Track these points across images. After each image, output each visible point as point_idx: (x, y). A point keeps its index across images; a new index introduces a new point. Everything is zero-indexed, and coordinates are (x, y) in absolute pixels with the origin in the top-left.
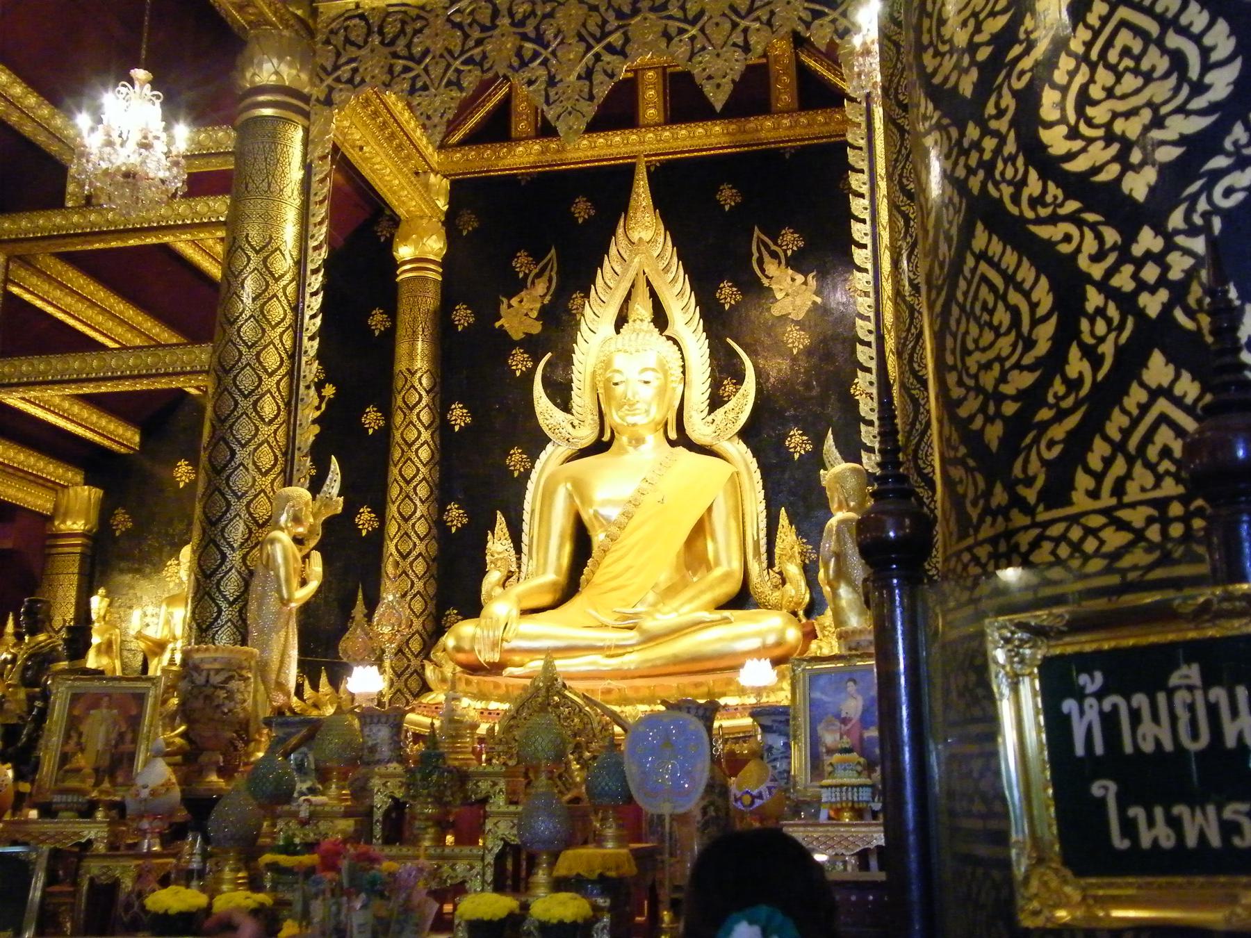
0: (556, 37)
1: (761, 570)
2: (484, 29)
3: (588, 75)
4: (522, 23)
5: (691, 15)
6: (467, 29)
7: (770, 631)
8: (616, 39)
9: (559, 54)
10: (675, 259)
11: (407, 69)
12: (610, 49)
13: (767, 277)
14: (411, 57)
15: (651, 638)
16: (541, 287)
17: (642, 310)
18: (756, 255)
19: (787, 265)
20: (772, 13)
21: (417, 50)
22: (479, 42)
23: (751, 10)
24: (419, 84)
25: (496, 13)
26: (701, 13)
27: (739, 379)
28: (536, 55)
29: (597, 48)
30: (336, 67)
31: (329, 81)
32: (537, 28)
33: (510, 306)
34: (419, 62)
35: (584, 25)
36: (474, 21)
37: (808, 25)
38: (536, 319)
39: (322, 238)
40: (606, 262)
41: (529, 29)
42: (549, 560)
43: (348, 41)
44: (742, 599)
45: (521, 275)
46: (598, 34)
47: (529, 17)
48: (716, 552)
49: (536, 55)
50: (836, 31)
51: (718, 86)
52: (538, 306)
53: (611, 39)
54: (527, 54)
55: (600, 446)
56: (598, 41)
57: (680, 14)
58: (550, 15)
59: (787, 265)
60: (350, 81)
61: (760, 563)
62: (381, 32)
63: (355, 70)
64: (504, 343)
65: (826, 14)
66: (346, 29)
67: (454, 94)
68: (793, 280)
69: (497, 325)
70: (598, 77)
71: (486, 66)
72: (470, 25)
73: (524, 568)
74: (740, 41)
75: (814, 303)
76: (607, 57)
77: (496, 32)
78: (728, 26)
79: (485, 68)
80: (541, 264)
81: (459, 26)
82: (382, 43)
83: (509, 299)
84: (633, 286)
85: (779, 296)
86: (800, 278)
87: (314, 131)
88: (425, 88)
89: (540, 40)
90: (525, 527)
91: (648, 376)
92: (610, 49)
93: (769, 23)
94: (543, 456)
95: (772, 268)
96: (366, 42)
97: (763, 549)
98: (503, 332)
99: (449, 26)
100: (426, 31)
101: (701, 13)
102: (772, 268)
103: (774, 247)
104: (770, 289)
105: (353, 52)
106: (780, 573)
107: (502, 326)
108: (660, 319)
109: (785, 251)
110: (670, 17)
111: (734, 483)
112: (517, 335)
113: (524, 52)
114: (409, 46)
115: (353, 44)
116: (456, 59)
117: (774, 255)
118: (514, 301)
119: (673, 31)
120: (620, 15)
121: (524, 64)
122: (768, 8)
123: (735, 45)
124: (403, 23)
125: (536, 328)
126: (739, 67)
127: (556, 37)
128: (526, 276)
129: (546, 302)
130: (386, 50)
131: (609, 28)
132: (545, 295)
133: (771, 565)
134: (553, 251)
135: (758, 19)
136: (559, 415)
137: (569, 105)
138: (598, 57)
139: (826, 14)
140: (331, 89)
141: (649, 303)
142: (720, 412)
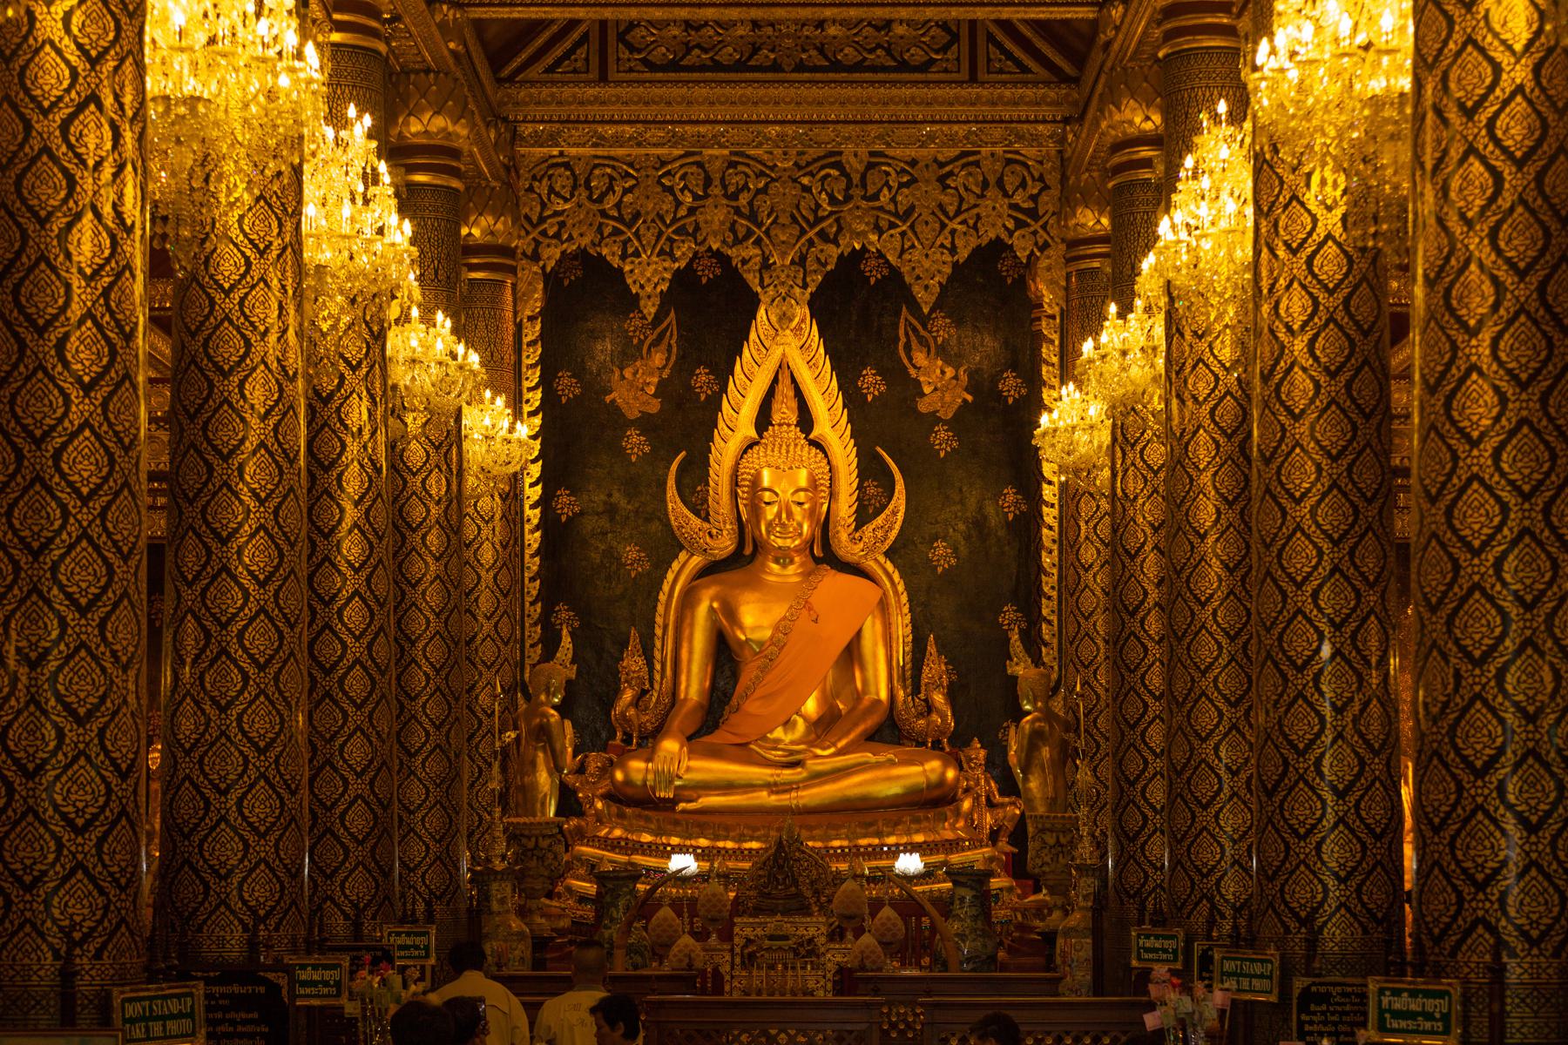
0: (769, 216)
1: (907, 695)
2: (696, 197)
3: (801, 261)
4: (734, 196)
5: (901, 209)
6: (678, 193)
7: (933, 770)
8: (829, 226)
9: (773, 233)
10: (822, 350)
11: (616, 232)
12: (822, 235)
13: (914, 366)
14: (620, 219)
16: (658, 359)
17: (785, 411)
18: (903, 340)
19: (937, 354)
20: (978, 217)
21: (627, 213)
22: (692, 211)
23: (958, 212)
24: (630, 250)
25: (708, 182)
26: (912, 208)
28: (750, 233)
29: (811, 234)
30: (542, 220)
31: (535, 234)
32: (750, 203)
33: (623, 378)
34: (629, 227)
35: (798, 207)
36: (685, 187)
37: (1011, 233)
38: (655, 396)
39: (537, 404)
40: (746, 350)
41: (743, 200)
42: (694, 684)
43: (551, 190)
44: (889, 731)
45: (635, 341)
46: (811, 218)
47: (742, 190)
48: (865, 682)
49: (750, 233)
50: (1036, 244)
51: (926, 287)
52: (656, 380)
53: (824, 225)
54: (741, 232)
56: (812, 226)
57: (891, 207)
58: (764, 190)
59: (937, 354)
60: (557, 236)
61: (905, 688)
62: (588, 187)
63: (562, 225)
64: (616, 420)
65: (1028, 225)
66: (550, 177)
67: (666, 264)
68: (943, 373)
69: (608, 399)
70: (811, 265)
71: (700, 238)
72: (682, 190)
73: (657, 686)
74: (947, 243)
75: (965, 400)
76: (820, 245)
77: (709, 201)
78: (937, 226)
79: (700, 238)
80: (658, 330)
81: (670, 190)
82: (590, 198)
83: (622, 369)
84: (775, 380)
85: (927, 390)
86: (950, 372)
87: (522, 287)
88: (637, 254)
89: (753, 217)
90: (658, 644)
91: (802, 496)
92: (822, 235)
93: (975, 227)
94: (676, 566)
95: (920, 358)
96: (572, 195)
97: (908, 674)
99: (659, 189)
100: (637, 192)
101: (912, 208)
102: (920, 358)
103: (922, 332)
104: (918, 384)
105: (561, 206)
106: (926, 701)
107: (613, 401)
108: (806, 421)
109: (935, 338)
110: (881, 209)
111: (883, 606)
112: (633, 414)
113: (738, 227)
114: (618, 206)
115: (558, 195)
116: (668, 227)
117: (923, 342)
118: (628, 373)
119: (883, 224)
120: (832, 200)
121: (738, 242)
122: (975, 211)
123: (942, 246)
124: (612, 178)
125: (654, 407)
126: (948, 270)
127: (769, 216)
128: (641, 342)
129: (665, 376)
130: (595, 207)
131: (820, 213)
132: (664, 367)
133: (916, 690)
134: (672, 314)
135: (964, 222)
136: (696, 521)
137: (783, 291)
138: (811, 243)
139: (1028, 225)
140: (537, 243)
141: (794, 404)
142: (868, 529)
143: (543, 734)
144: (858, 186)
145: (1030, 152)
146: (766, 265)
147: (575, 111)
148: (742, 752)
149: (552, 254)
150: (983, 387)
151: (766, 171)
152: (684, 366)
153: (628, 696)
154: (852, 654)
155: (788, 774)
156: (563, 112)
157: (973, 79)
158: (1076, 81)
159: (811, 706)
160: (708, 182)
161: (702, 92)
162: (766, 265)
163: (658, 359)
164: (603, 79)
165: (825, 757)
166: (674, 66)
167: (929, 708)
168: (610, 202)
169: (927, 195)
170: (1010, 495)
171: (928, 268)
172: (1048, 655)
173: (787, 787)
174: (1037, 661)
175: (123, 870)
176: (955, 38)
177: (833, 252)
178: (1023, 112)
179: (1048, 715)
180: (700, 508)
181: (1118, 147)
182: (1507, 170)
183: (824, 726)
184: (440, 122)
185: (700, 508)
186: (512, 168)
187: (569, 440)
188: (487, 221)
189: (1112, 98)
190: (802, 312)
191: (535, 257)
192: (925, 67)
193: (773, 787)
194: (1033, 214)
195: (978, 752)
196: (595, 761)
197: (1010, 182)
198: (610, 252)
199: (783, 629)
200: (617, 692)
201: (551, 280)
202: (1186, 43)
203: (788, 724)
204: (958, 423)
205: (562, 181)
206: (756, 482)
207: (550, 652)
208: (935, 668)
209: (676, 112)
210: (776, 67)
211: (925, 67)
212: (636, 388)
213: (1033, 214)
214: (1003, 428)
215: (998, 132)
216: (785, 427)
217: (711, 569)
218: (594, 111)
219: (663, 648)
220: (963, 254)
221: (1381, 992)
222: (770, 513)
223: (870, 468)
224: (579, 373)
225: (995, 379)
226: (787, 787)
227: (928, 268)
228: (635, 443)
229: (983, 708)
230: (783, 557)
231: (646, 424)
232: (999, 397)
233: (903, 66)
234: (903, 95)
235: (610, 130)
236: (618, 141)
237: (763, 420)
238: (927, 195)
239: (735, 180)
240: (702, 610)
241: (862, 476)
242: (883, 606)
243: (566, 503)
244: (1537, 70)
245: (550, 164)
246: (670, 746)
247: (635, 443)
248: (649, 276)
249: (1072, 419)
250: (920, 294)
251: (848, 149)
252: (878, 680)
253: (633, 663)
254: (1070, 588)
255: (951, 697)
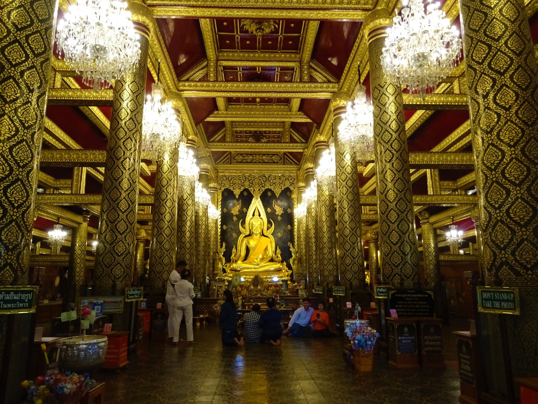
3: (259, 190)
8: (263, 185)
15: (261, 267)
16: (238, 206)
17: (257, 213)
27: (272, 225)
41: (251, 181)
42: (243, 253)
44: (272, 260)
55: (250, 235)
89: (252, 184)
95: (276, 206)
98: (232, 214)
102: (276, 206)
108: (260, 215)
111: (271, 242)
143: (220, 259)
144: (267, 179)
145: (292, 175)
146: (254, 190)
147: (227, 168)
148: (250, 263)
149: (223, 189)
150: (285, 210)
151: (254, 177)
152: (242, 208)
153: (233, 255)
154: (266, 249)
155: (257, 266)
156: (225, 168)
157: (284, 164)
158: (299, 165)
159: (260, 256)
160: (246, 179)
161: (245, 166)
162: (254, 190)
163: (238, 206)
164: (231, 164)
165: (263, 264)
166: (241, 162)
167: (278, 257)
168: (231, 181)
169: (277, 181)
170: (289, 226)
171: (278, 191)
172: (296, 247)
173: (257, 268)
174: (294, 248)
175: (128, 264)
176: (281, 159)
177: (264, 189)
178: (291, 169)
179: (296, 256)
180: (244, 228)
181: (306, 170)
182: (393, 133)
183: (262, 259)
184: (206, 165)
185: (244, 228)
186: (217, 177)
187: (226, 217)
188: (214, 184)
189: (306, 162)
190: (259, 199)
191: (220, 189)
192: (277, 163)
193: (255, 268)
194: (293, 183)
195: (285, 263)
196: (228, 265)
197: (290, 179)
198: (231, 188)
199: (256, 245)
200: (231, 254)
201: (223, 193)
202: (319, 147)
203: (257, 259)
204: (282, 216)
205: (225, 179)
206: (252, 224)
207: (221, 247)
208: (279, 251)
209: (241, 169)
210: (256, 162)
211: (277, 163)
212: (235, 210)
213: (293, 183)
214: (288, 218)
215: (287, 172)
216: (256, 214)
217: (246, 236)
218: (229, 168)
219: (239, 248)
220: (283, 189)
221: (377, 288)
222: (254, 228)
223: (269, 222)
224: (227, 208)
225: (287, 209)
226: (257, 268)
227: (278, 191)
228: (235, 219)
229: (286, 256)
230: (256, 234)
231: (237, 216)
232: (287, 212)
233: (274, 162)
234: (274, 166)
235: (231, 171)
236: (233, 173)
237: (253, 215)
238: (277, 181)
239: (250, 178)
240: (244, 242)
241: (268, 223)
242: (271, 242)
243: (225, 227)
244: (397, 116)
245: (223, 176)
246: (239, 262)
247: (235, 219)
248: (237, 192)
249: (300, 212)
250: (276, 195)
251: (266, 174)
252: (270, 253)
253: (234, 250)
254: (299, 238)
255: (281, 255)
